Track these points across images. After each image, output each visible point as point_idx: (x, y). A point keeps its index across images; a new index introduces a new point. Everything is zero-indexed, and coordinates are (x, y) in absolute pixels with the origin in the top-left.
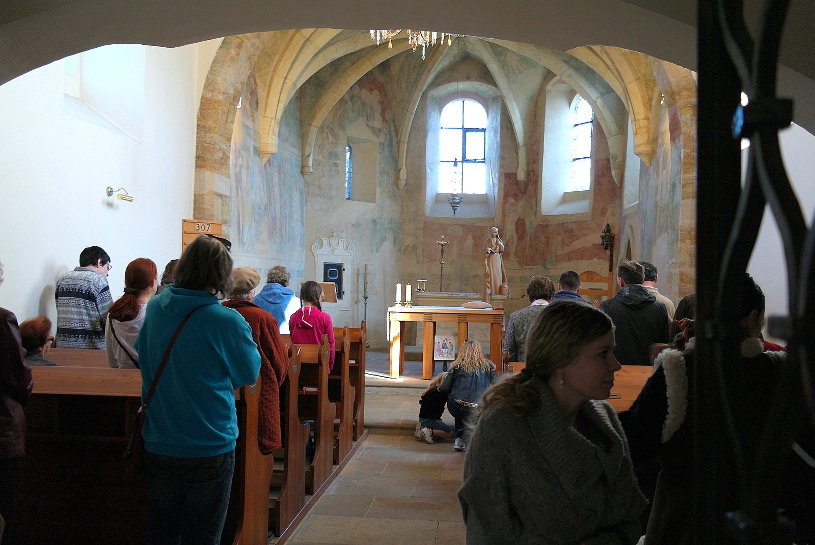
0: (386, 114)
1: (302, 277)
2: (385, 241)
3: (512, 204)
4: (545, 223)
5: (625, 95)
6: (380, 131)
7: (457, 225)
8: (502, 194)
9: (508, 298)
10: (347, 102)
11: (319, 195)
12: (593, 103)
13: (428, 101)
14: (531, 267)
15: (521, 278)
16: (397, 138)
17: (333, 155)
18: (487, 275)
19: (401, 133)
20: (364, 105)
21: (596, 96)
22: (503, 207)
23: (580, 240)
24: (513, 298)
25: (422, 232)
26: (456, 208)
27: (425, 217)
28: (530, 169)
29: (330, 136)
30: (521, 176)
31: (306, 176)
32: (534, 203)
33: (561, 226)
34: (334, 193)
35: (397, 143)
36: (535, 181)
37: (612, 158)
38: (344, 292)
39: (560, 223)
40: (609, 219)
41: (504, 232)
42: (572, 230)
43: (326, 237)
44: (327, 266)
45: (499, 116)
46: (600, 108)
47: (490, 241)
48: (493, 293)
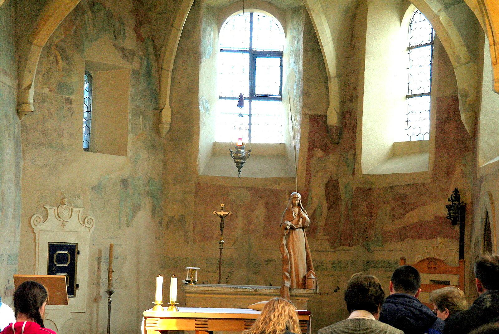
0: (142, 29)
1: (16, 264)
2: (140, 211)
3: (320, 158)
4: (366, 186)
5: (481, 9)
6: (133, 53)
7: (243, 188)
8: (307, 144)
9: (315, 293)
10: (84, 12)
11: (43, 144)
12: (433, 19)
13: (201, 12)
14: (347, 247)
15: (334, 263)
16: (158, 63)
17: (63, 87)
18: (286, 261)
19: (164, 56)
20: (109, 15)
21: (439, 9)
22: (308, 163)
23: (417, 210)
24: (323, 292)
26: (241, 165)
27: (198, 176)
28: (346, 110)
29: (59, 58)
30: (333, 119)
31: (23, 118)
32: (350, 157)
33: (389, 190)
34: (66, 141)
35: (158, 71)
36: (352, 126)
37: (462, 96)
38: (77, 286)
39: (387, 186)
40: (458, 181)
41: (310, 197)
42: (405, 196)
43: (52, 205)
44: (53, 248)
45: (302, 35)
46: (445, 26)
47: (289, 212)
48: (295, 286)
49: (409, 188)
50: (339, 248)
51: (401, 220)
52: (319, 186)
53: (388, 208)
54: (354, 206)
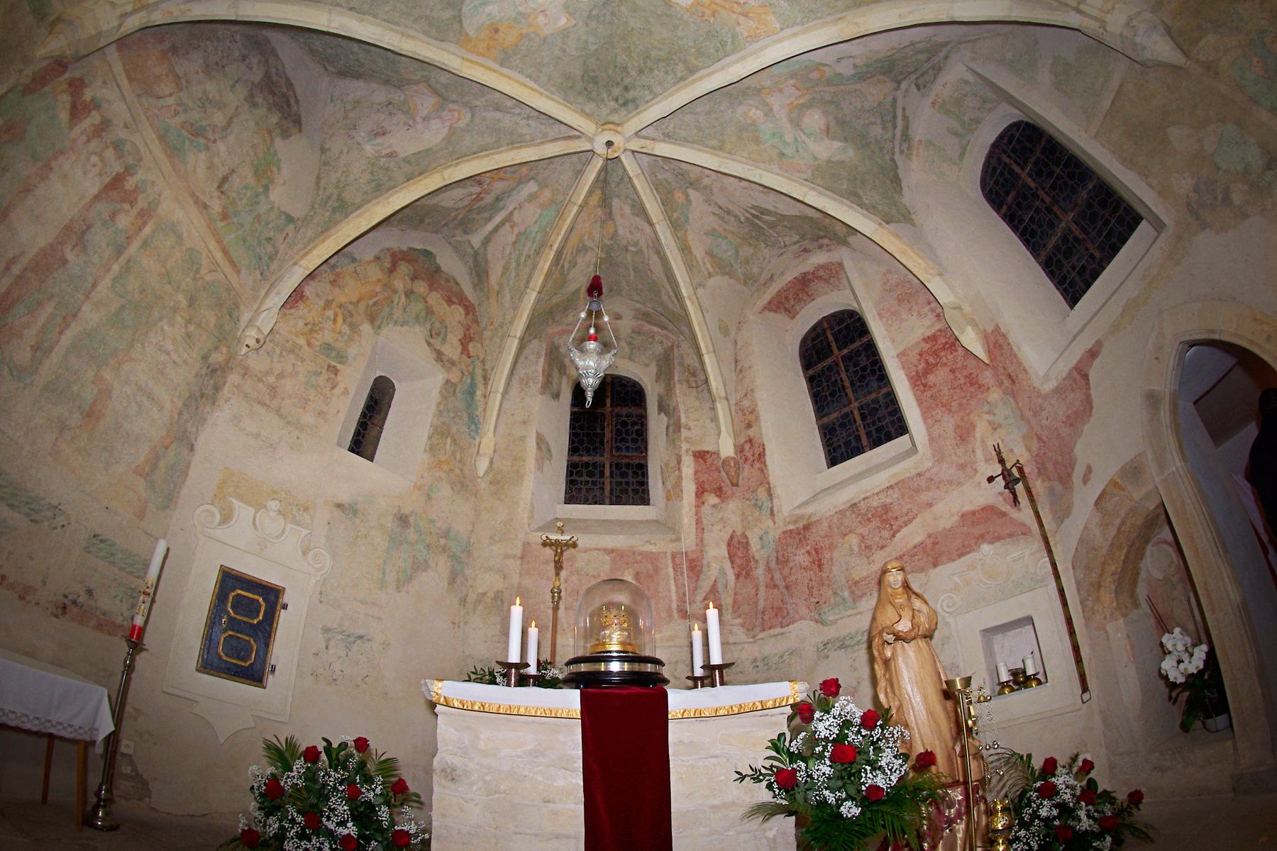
2: (425, 570)
3: (714, 506)
4: (801, 525)
6: (453, 363)
15: (755, 660)
20: (430, 311)
25: (518, 562)
29: (340, 320)
30: (727, 448)
33: (848, 513)
41: (705, 562)
42: (886, 508)
49: (891, 491)
50: (762, 635)
51: (887, 549)
52: (718, 545)
53: (853, 540)
54: (782, 561)
